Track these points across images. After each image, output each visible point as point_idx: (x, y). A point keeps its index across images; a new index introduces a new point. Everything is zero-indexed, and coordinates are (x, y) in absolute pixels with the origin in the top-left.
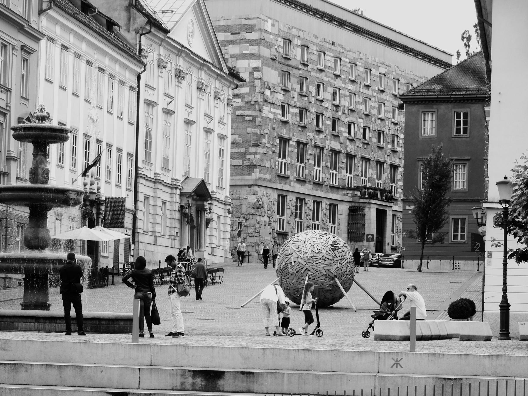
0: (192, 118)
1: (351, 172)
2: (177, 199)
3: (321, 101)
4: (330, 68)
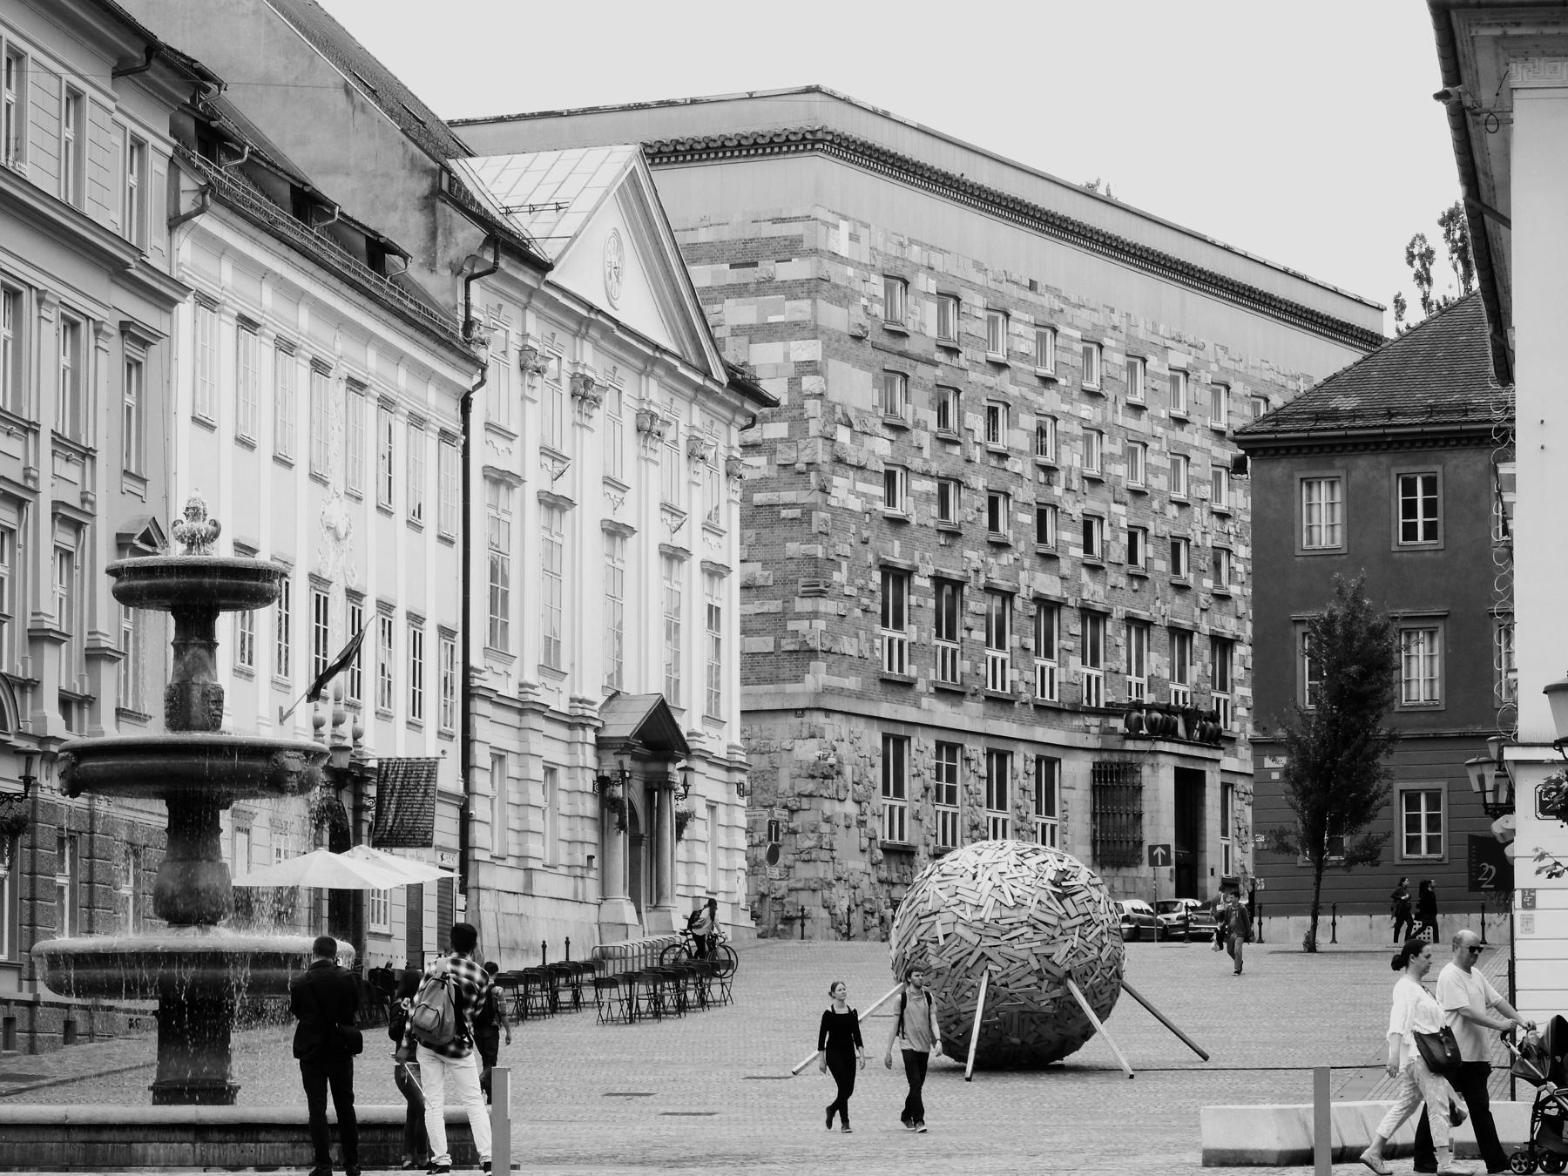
0: (625, 516)
1: (1095, 663)
2: (588, 757)
3: (1003, 456)
4: (1024, 356)
